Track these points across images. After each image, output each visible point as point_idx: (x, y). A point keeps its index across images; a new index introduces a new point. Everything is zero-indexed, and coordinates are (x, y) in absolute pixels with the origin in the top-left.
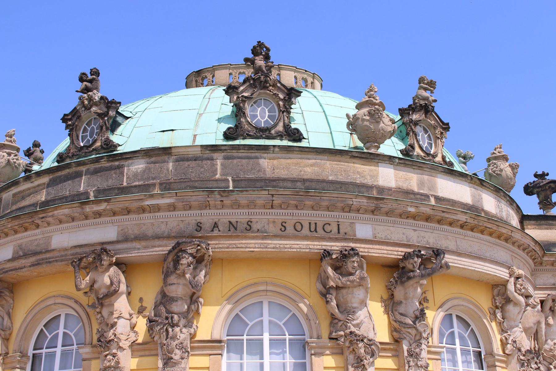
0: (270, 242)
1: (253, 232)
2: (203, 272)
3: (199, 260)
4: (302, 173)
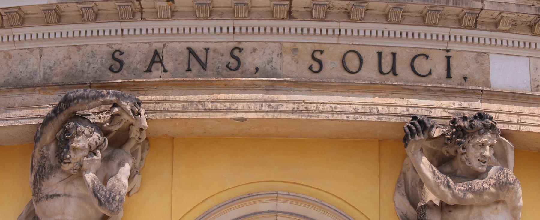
0: (283, 97)
2: (126, 169)
3: (117, 140)
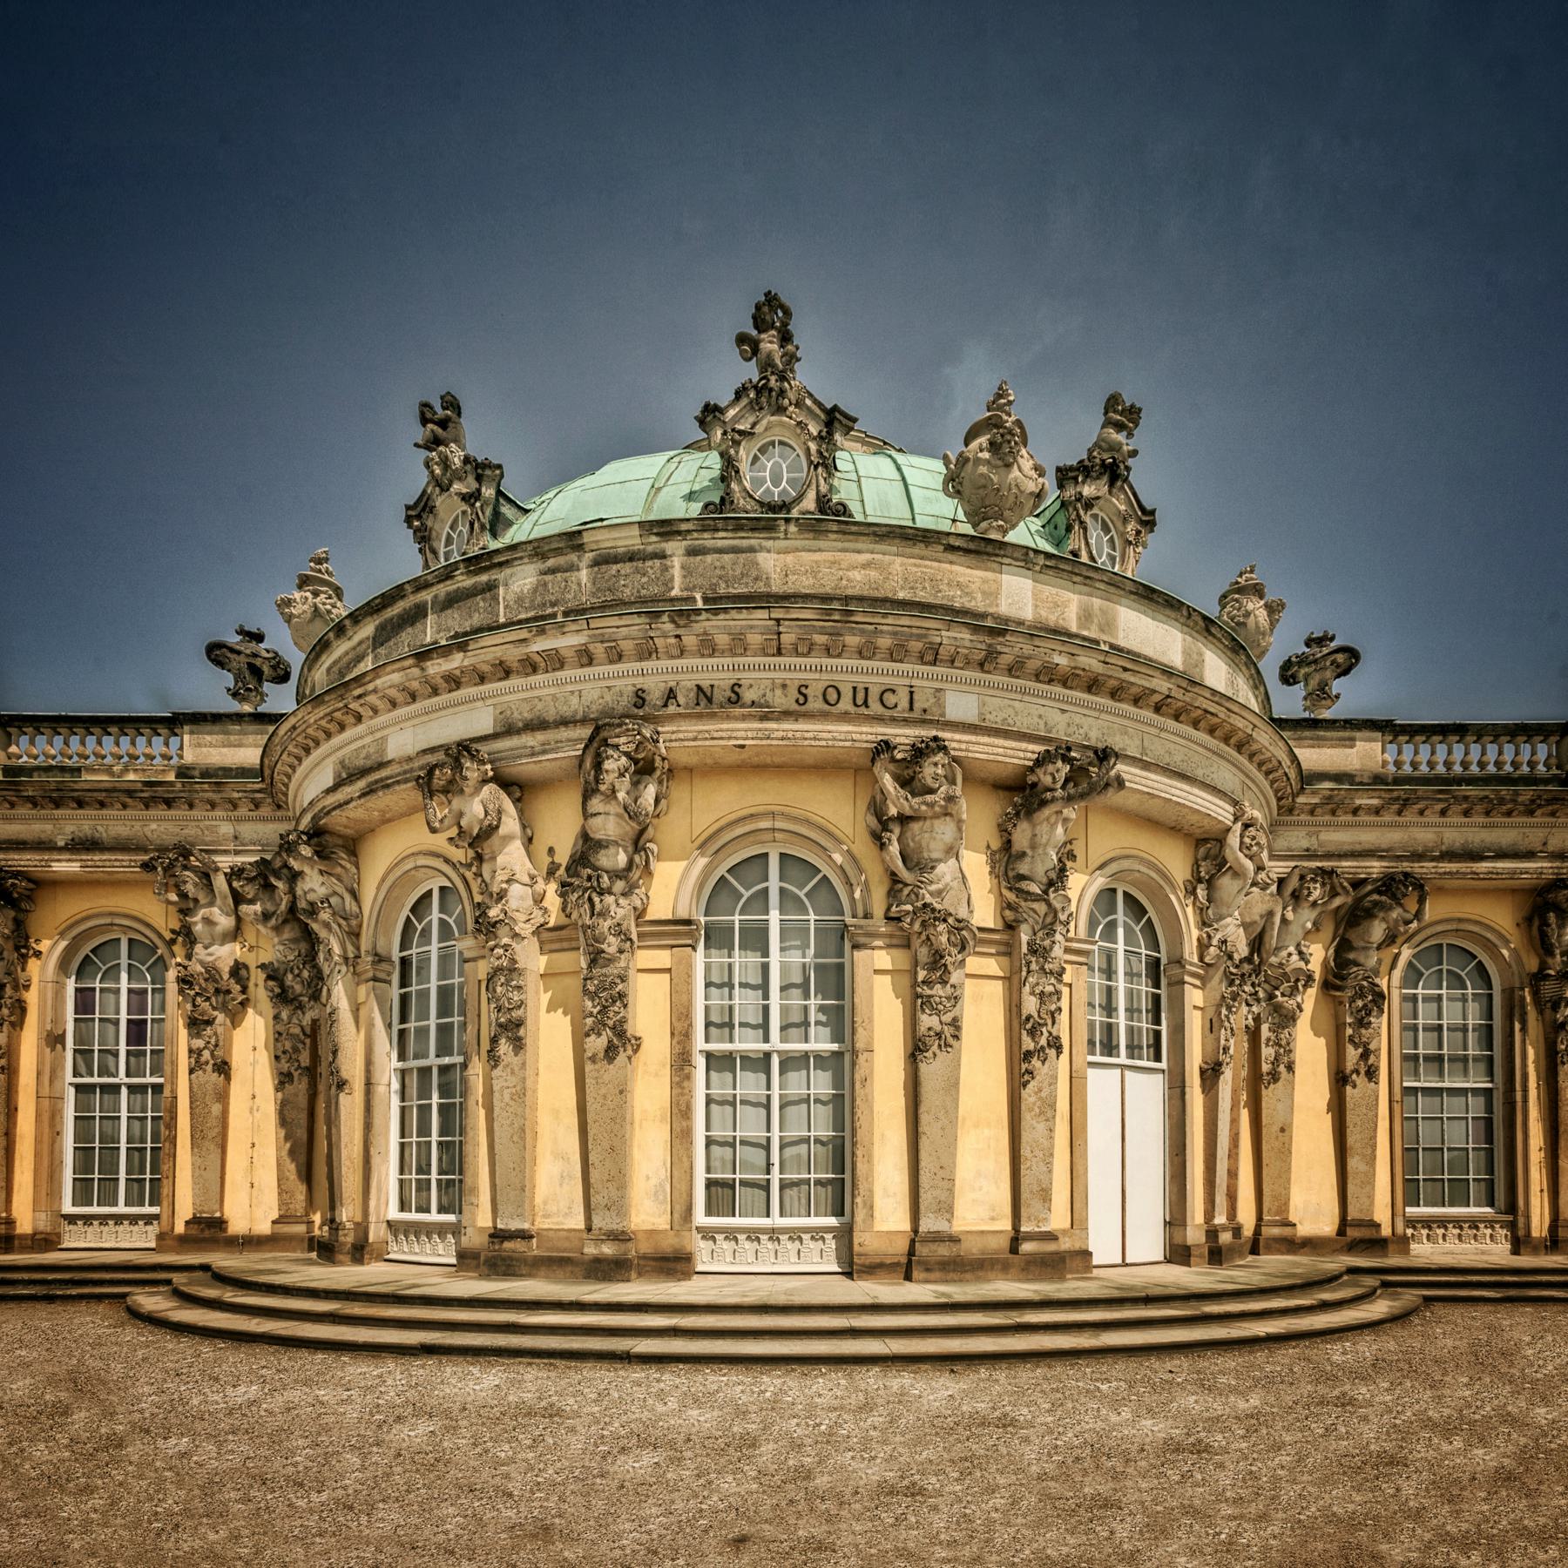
3: (643, 769)
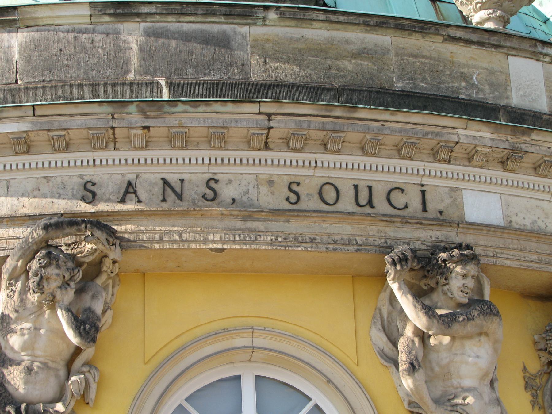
1: (219, 205)
4: (333, 72)
